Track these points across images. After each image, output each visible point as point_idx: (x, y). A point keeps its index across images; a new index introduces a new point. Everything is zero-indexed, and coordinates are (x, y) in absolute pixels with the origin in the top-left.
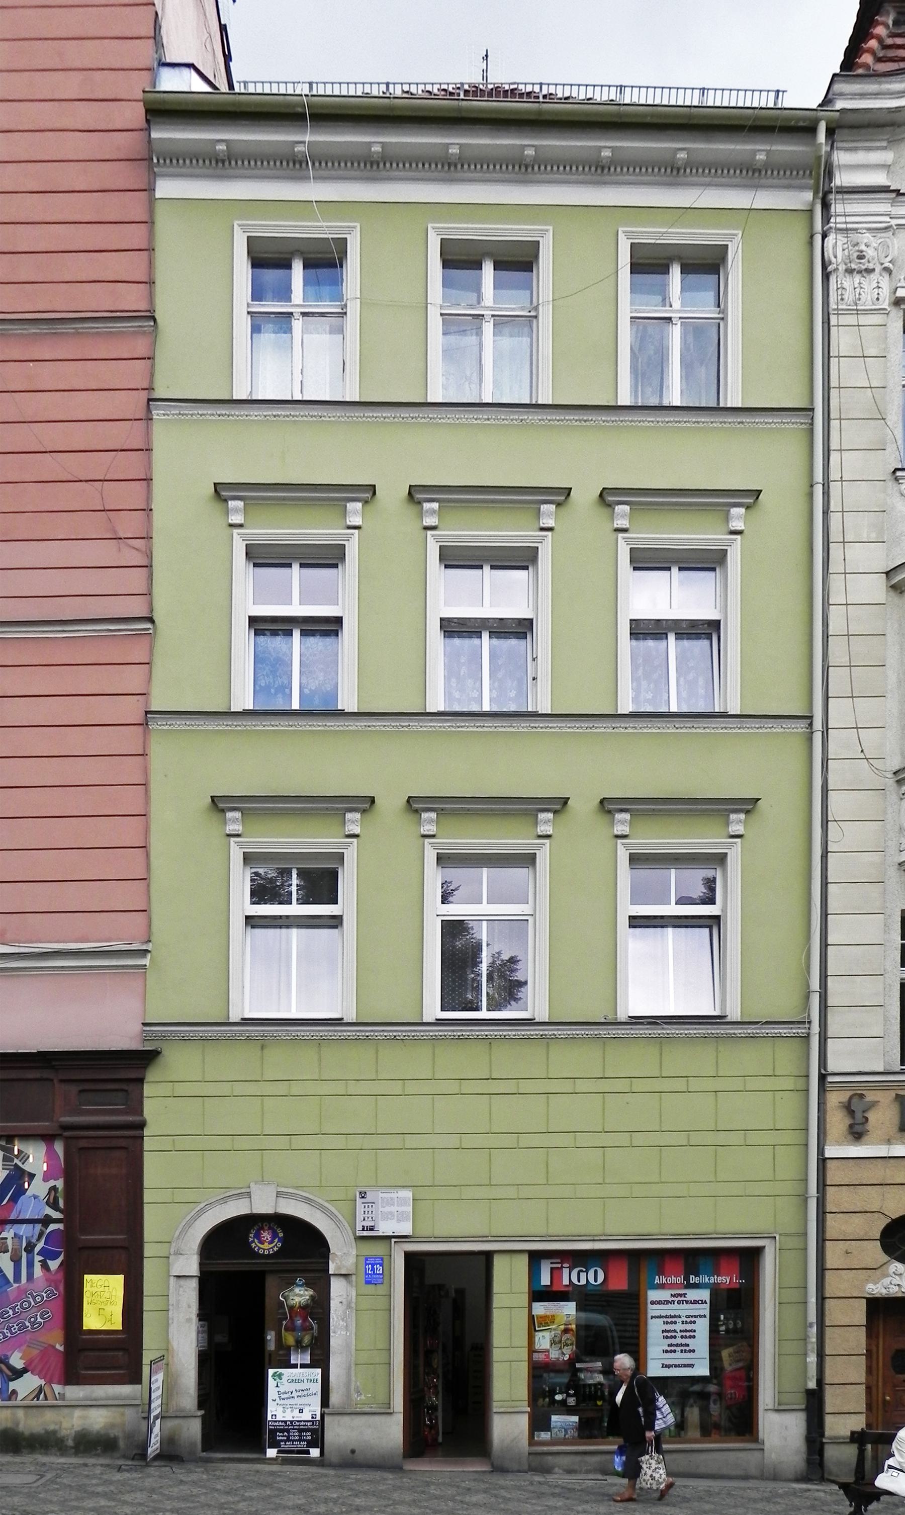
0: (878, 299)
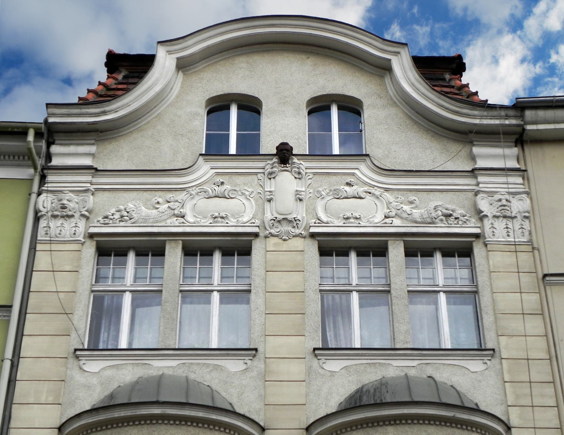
0: (75, 234)
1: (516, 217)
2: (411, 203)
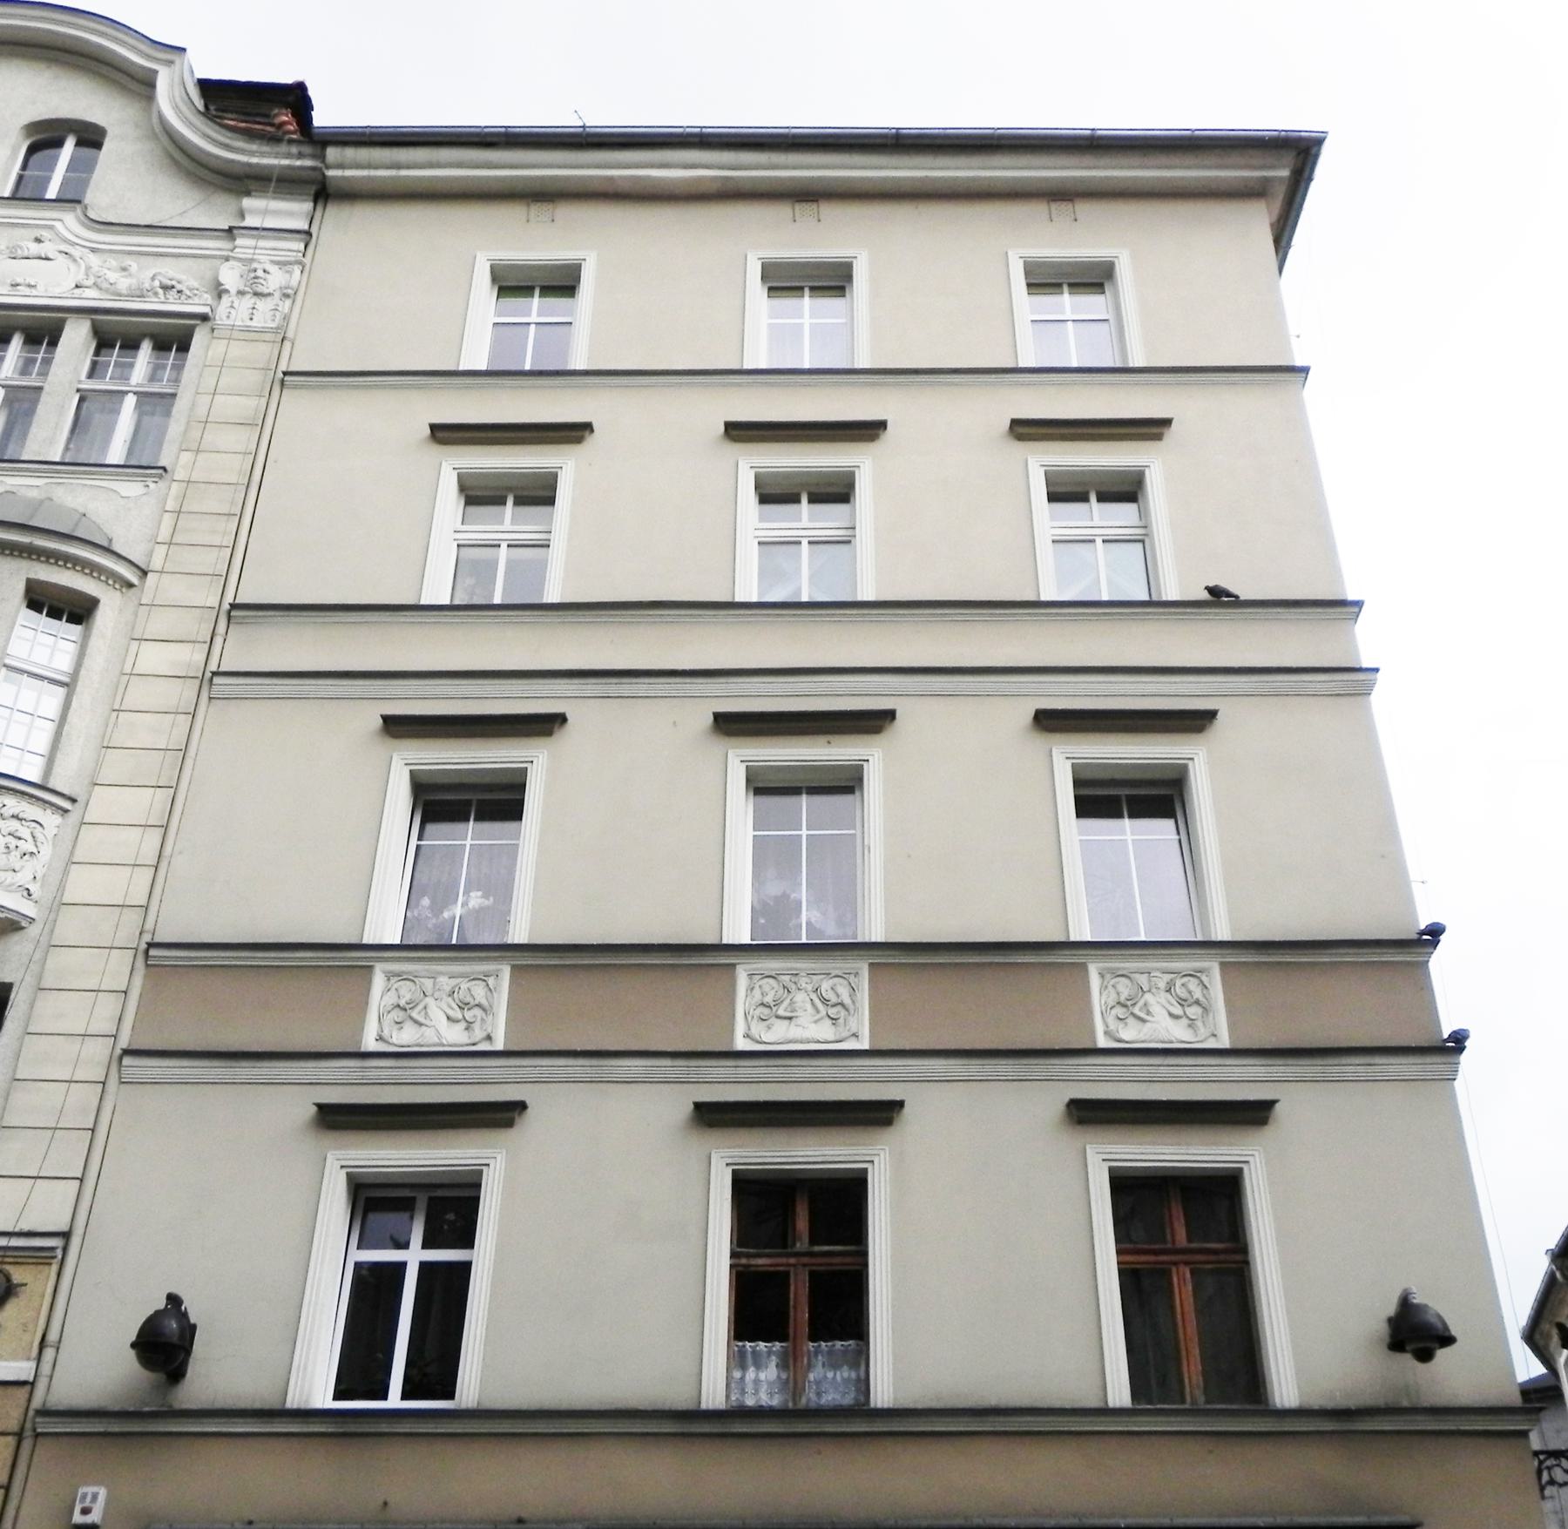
2: (124, 269)
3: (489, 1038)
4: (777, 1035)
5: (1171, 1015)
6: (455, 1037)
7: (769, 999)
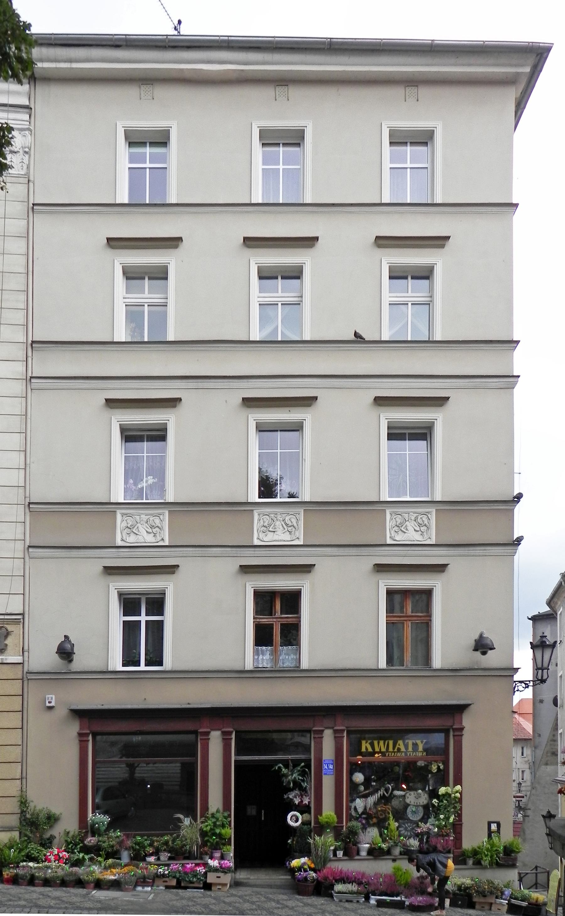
1: (18, 152)
3: (163, 539)
4: (269, 539)
5: (415, 530)
6: (150, 539)
7: (266, 524)
